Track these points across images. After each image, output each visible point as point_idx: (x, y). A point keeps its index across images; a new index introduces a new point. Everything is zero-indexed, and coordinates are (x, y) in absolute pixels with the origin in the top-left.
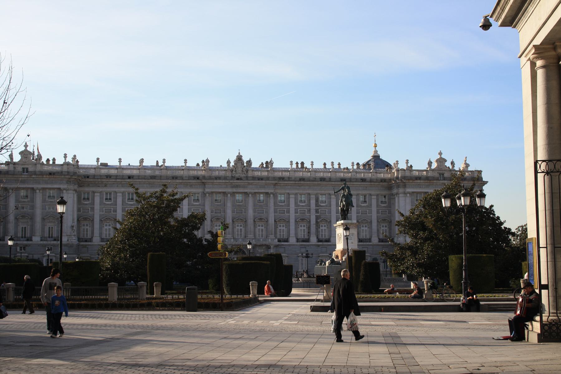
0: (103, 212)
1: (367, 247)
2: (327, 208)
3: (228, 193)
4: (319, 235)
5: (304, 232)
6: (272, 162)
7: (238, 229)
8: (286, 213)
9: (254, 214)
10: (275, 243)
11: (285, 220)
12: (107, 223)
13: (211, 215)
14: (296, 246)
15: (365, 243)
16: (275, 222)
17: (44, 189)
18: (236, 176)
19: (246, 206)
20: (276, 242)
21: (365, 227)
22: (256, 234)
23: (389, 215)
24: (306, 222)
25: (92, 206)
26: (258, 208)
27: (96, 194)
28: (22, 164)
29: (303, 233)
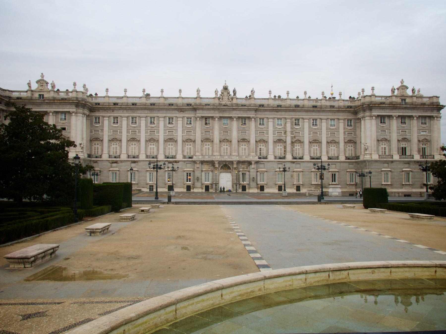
1: (335, 164)
3: (216, 118)
4: (294, 153)
5: (281, 151)
6: (254, 91)
7: (224, 148)
8: (266, 135)
10: (256, 160)
11: (265, 141)
12: (114, 142)
15: (333, 160)
16: (256, 143)
17: (57, 113)
20: (256, 159)
22: (240, 152)
23: (354, 136)
24: (282, 142)
25: (102, 128)
26: (242, 130)
28: (39, 92)
29: (280, 151)
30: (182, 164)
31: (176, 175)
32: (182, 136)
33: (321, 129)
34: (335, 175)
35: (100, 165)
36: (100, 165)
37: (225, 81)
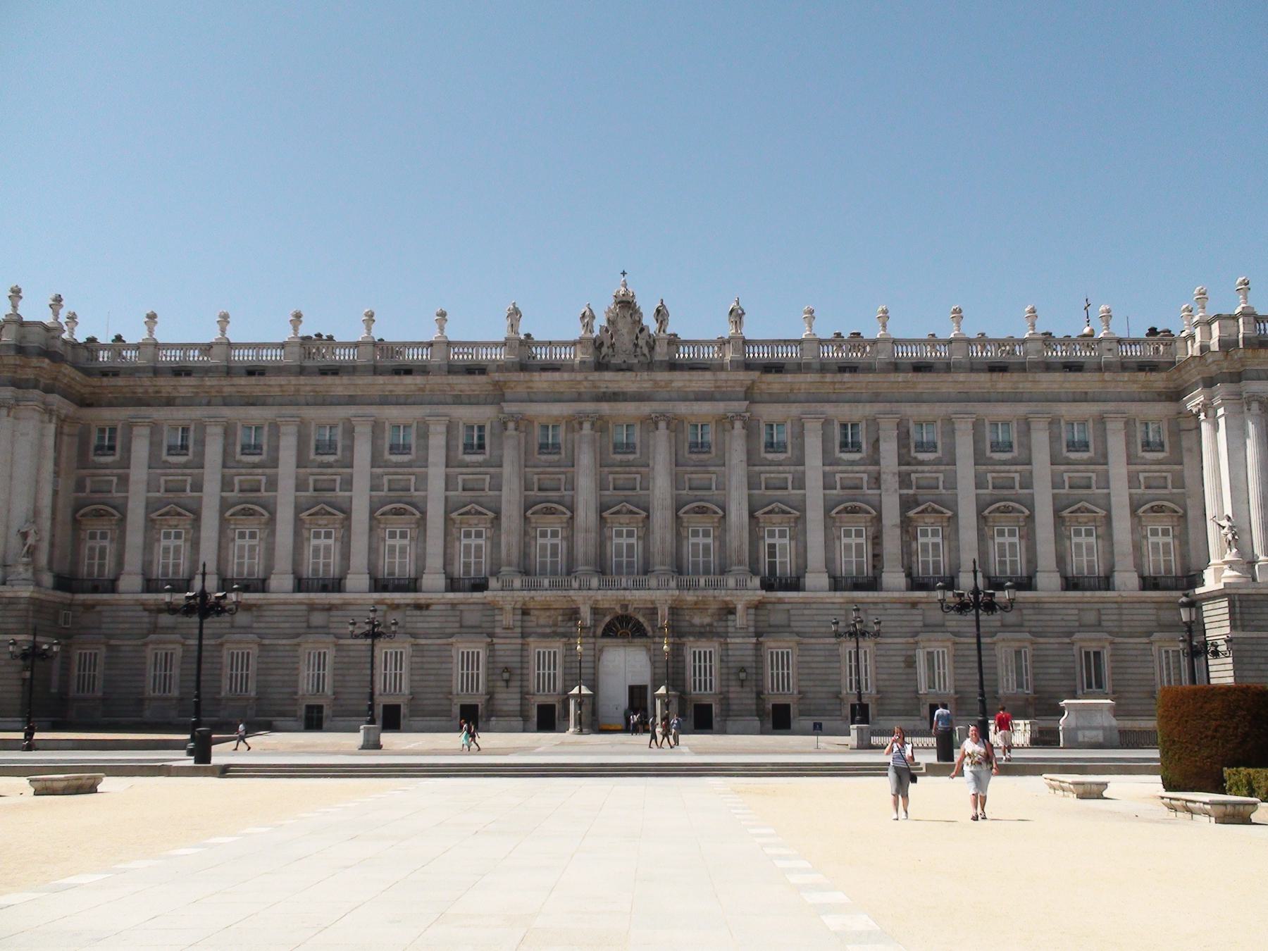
0: (159, 491)
2: (942, 468)
4: (915, 565)
5: (859, 554)
8: (793, 489)
9: (675, 492)
13: (525, 496)
14: (830, 606)
15: (1088, 594)
18: (612, 362)
19: (648, 466)
21: (1086, 535)
27: (136, 431)
30: (445, 613)
31: (418, 660)
32: (446, 498)
33: (1030, 463)
34: (1097, 654)
35: (109, 620)
36: (109, 620)
37: (624, 273)
